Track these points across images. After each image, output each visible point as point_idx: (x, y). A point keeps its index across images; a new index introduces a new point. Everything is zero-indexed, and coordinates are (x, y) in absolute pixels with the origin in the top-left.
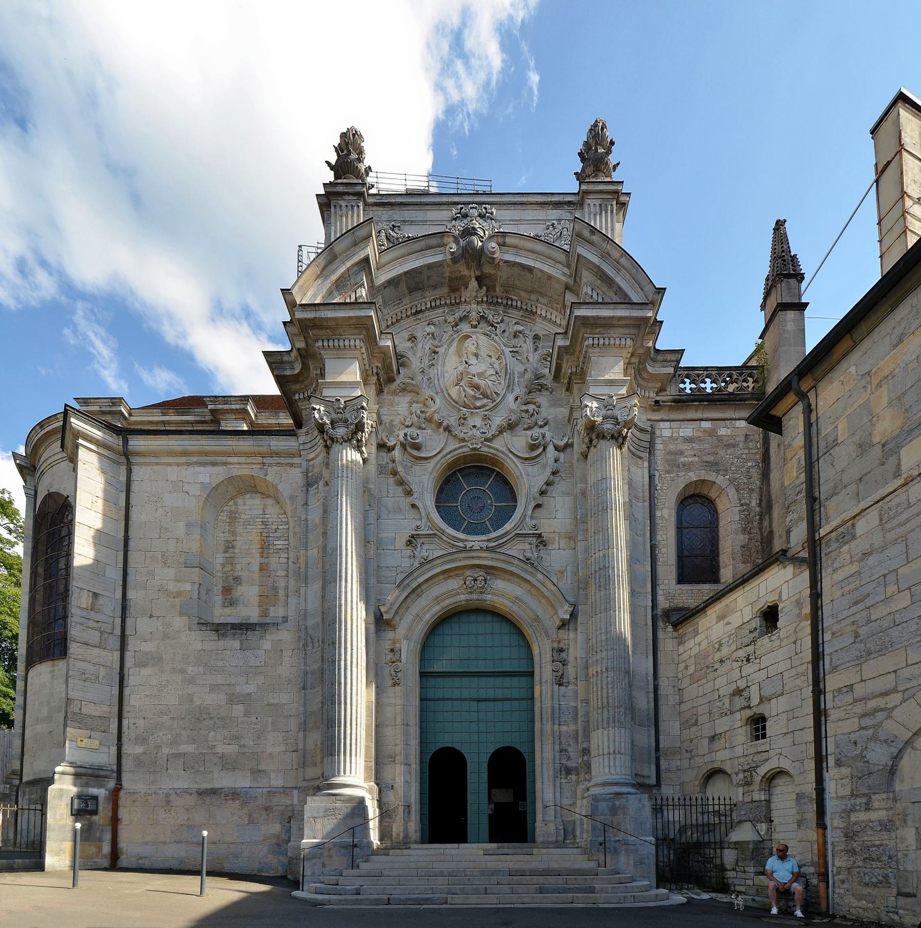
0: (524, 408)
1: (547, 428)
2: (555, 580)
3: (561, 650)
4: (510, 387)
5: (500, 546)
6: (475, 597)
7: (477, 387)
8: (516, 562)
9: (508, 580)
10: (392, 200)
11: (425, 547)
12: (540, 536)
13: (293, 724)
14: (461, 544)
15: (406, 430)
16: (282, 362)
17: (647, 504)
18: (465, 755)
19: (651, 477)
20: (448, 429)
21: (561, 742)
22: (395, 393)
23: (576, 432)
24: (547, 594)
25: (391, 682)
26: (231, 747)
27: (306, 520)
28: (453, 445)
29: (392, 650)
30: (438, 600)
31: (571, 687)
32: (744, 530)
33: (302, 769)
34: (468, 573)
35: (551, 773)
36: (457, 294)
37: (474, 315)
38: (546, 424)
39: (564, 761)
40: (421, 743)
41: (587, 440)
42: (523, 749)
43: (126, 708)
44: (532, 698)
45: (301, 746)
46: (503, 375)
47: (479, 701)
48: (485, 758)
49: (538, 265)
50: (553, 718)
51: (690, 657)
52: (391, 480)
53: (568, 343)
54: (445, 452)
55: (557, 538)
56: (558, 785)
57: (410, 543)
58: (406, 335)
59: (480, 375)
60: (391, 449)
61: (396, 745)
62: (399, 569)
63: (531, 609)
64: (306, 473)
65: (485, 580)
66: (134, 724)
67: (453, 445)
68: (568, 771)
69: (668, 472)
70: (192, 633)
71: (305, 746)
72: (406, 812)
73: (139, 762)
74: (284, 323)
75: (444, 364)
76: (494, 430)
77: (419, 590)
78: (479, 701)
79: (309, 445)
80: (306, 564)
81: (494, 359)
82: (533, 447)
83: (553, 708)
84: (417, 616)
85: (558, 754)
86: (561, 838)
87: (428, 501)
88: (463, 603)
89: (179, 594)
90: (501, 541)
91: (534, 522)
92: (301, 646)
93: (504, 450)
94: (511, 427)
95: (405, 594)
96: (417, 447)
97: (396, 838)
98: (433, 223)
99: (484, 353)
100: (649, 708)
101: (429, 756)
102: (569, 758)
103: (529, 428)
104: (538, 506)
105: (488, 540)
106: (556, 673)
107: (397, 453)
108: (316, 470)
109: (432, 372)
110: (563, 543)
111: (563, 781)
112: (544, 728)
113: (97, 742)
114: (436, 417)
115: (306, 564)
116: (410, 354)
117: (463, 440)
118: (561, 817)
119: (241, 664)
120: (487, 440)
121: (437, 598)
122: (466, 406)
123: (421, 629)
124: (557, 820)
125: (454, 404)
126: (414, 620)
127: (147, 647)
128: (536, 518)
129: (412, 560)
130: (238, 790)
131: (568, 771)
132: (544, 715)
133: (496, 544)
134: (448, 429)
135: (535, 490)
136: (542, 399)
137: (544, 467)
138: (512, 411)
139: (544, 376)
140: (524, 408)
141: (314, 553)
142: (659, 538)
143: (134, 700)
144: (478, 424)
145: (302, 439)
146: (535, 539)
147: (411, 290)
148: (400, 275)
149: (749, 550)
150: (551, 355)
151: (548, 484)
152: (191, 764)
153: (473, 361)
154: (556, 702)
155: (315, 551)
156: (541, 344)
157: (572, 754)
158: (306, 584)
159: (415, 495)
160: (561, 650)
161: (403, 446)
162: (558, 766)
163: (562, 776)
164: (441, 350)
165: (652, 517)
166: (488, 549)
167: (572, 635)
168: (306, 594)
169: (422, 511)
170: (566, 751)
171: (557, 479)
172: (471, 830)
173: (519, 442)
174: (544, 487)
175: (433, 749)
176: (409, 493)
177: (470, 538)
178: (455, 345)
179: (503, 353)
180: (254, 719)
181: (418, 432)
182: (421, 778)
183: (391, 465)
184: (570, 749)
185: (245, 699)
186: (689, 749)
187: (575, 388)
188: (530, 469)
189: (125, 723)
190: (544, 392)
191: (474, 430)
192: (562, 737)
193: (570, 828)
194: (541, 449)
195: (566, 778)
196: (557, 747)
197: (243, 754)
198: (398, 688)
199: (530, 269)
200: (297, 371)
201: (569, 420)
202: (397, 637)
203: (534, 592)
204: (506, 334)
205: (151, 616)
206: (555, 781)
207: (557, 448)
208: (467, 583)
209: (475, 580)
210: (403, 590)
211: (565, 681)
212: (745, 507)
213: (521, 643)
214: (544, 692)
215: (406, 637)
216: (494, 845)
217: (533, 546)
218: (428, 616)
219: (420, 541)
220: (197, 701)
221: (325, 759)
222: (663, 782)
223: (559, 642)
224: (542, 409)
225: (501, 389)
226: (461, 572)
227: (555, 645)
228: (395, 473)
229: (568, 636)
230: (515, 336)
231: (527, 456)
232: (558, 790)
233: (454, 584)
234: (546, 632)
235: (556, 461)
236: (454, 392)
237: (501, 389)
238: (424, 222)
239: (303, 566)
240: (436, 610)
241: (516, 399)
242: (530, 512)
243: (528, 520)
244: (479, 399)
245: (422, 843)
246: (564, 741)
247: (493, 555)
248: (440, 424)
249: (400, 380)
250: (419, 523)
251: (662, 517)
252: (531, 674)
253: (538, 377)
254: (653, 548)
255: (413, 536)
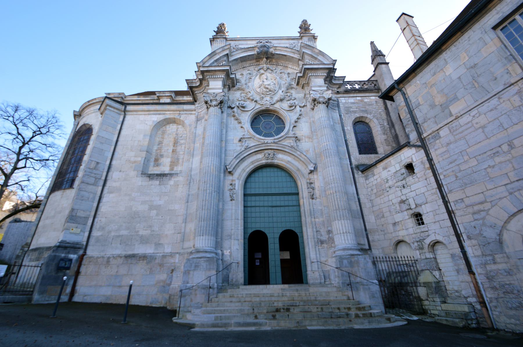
0: (286, 94)
1: (295, 101)
2: (305, 154)
3: (311, 183)
4: (280, 88)
5: (279, 141)
6: (269, 161)
7: (267, 88)
8: (287, 147)
9: (284, 154)
10: (236, 39)
11: (247, 142)
12: (296, 137)
13: (180, 220)
14: (262, 141)
15: (239, 102)
16: (192, 82)
17: (340, 125)
18: (267, 234)
19: (340, 116)
20: (256, 101)
21: (316, 227)
22: (235, 91)
23: (308, 102)
24: (302, 160)
25: (230, 199)
26: (147, 231)
27: (196, 133)
28: (259, 106)
29: (231, 184)
30: (252, 163)
31: (318, 200)
32: (384, 134)
33: (182, 243)
34: (266, 151)
35: (313, 243)
36: (259, 62)
37: (265, 68)
38: (295, 99)
39: (319, 237)
40: (244, 228)
41: (313, 104)
42: (297, 231)
43: (98, 213)
44: (299, 205)
45: (183, 231)
46: (277, 84)
47: (273, 207)
48: (278, 236)
49: (288, 54)
50: (311, 215)
51: (373, 185)
52: (233, 118)
53: (301, 75)
54: (255, 109)
55: (304, 138)
56: (317, 250)
57: (240, 141)
58: (239, 74)
59: (269, 85)
60: (232, 108)
61: (232, 230)
62: (235, 151)
63: (296, 166)
64: (197, 117)
65: (274, 155)
66: (100, 220)
67: (258, 106)
68: (322, 242)
69: (347, 114)
70: (138, 178)
71: (185, 230)
72: (237, 266)
73: (98, 240)
74: (195, 72)
75: (254, 82)
76: (274, 101)
77: (244, 159)
78: (273, 207)
79: (199, 107)
80: (194, 149)
81: (273, 80)
82: (291, 107)
83: (310, 210)
84: (243, 169)
85: (315, 233)
86: (323, 281)
87: (247, 125)
88: (264, 164)
89: (135, 162)
90: (280, 139)
91: (293, 132)
92: (188, 183)
93: (279, 108)
94: (281, 100)
95: (238, 161)
96: (243, 107)
97: (231, 282)
98: (250, 44)
99: (269, 78)
100: (357, 209)
101: (249, 235)
102: (321, 235)
103: (288, 101)
104: (295, 126)
105: (274, 139)
106: (310, 194)
107: (235, 110)
108: (202, 115)
109: (250, 84)
110: (307, 140)
111: (320, 247)
112: (306, 220)
113: (80, 230)
114: (251, 98)
115: (194, 149)
116: (241, 79)
117: (262, 105)
118: (321, 268)
119: (158, 191)
120: (272, 105)
121: (252, 162)
122: (263, 94)
123: (244, 175)
124: (319, 270)
125: (258, 93)
126: (242, 171)
127: (115, 184)
128: (294, 131)
129: (241, 147)
130: (147, 255)
131: (322, 242)
132: (306, 214)
133: (278, 140)
134: (256, 101)
135: (293, 121)
136: (293, 91)
137: (296, 113)
138: (282, 95)
139: (293, 85)
140: (286, 94)
141: (197, 145)
142: (347, 137)
143: (103, 208)
144: (268, 100)
145: (196, 106)
146: (294, 139)
147: (242, 62)
148: (238, 58)
149: (388, 141)
150: (295, 79)
151: (298, 119)
152: (125, 241)
153: (265, 80)
154: (311, 207)
155: (199, 144)
156: (290, 75)
157: (323, 233)
158: (193, 157)
159: (243, 124)
160: (311, 183)
161: (238, 107)
162: (316, 240)
163: (319, 245)
164: (253, 78)
165: (343, 130)
166: (274, 143)
167: (315, 176)
168: (192, 161)
169: (246, 129)
170: (319, 231)
171: (301, 117)
172: (272, 276)
173: (285, 105)
174: (297, 120)
175: (250, 231)
176: (240, 123)
177: (266, 138)
178: (258, 76)
179: (276, 78)
180: (160, 217)
181: (244, 102)
182: (244, 247)
183: (232, 114)
184: (321, 230)
185: (158, 208)
186: (382, 230)
187: (306, 88)
188: (290, 114)
189: (96, 220)
190: (293, 89)
191: (267, 102)
192: (317, 225)
193: (327, 275)
194: (294, 107)
195: (321, 246)
196: (315, 230)
197: (152, 235)
198: (233, 202)
199: (285, 55)
200: (197, 85)
201: (304, 98)
202: (234, 179)
203: (296, 158)
204: (277, 73)
205: (120, 171)
206: (315, 248)
207: (300, 107)
208: (266, 156)
209: (269, 154)
210: (237, 159)
211: (315, 197)
212: (382, 126)
213: (292, 180)
214: (305, 202)
215: (238, 179)
216: (286, 286)
217: (294, 141)
218: (248, 170)
219: (244, 140)
220: (134, 209)
221: (196, 238)
222: (372, 248)
223: (310, 180)
224: (293, 94)
225: (277, 89)
226: (263, 151)
227: (308, 181)
228: (234, 116)
229: (314, 177)
230: (281, 73)
231: (288, 109)
232: (318, 252)
233: (260, 156)
234: (303, 175)
235: (300, 111)
236: (258, 90)
237: (277, 89)
238: (247, 44)
239: (192, 150)
240: (252, 167)
241: (283, 92)
242: (291, 129)
243: (291, 131)
244: (268, 92)
245: (245, 284)
246: (318, 226)
247: (277, 145)
248: (253, 100)
249: (236, 87)
250: (244, 133)
251: (348, 130)
252: (298, 194)
253: (290, 85)
254: (346, 141)
255: (241, 138)
